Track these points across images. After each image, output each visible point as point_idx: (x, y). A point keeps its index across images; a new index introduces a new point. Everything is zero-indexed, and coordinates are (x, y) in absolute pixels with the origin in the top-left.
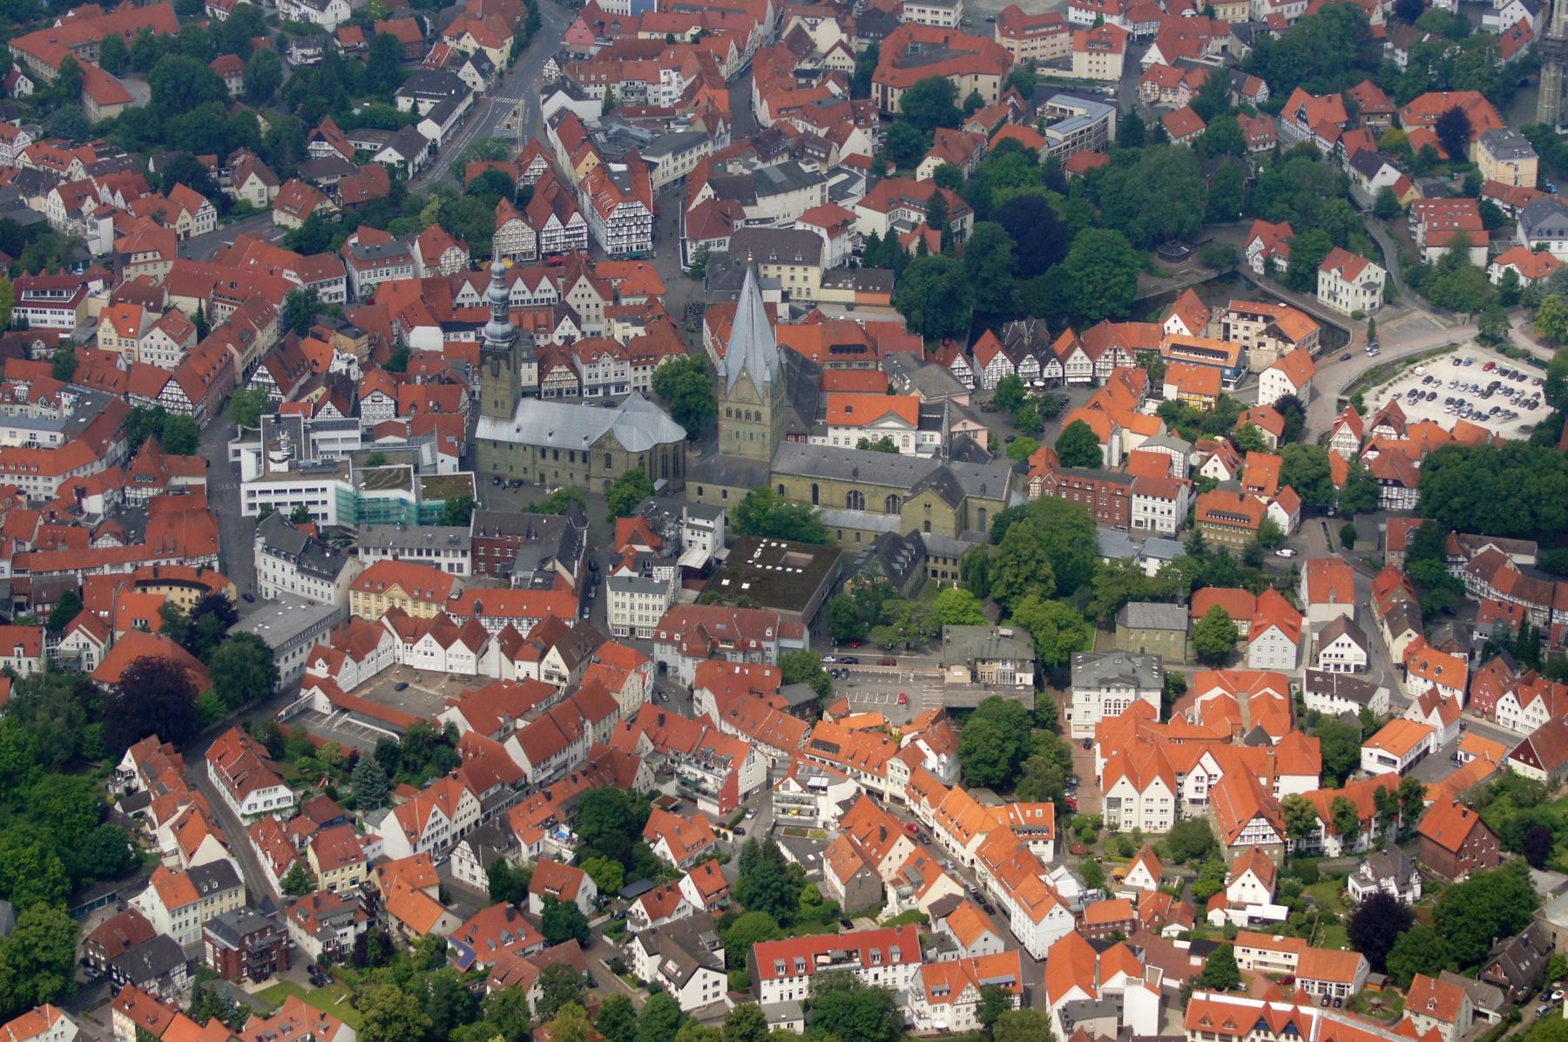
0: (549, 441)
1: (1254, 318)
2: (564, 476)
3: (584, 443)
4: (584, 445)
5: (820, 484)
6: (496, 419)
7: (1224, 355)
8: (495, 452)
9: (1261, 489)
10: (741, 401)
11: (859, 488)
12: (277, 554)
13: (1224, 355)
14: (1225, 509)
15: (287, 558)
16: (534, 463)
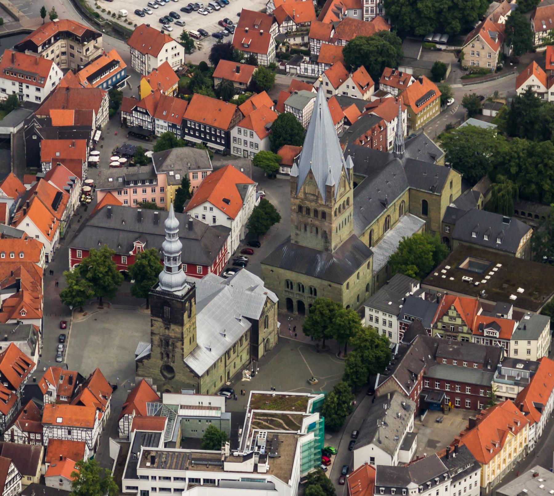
0: (229, 340)
1: (48, 43)
2: (238, 361)
3: (241, 323)
4: (245, 326)
5: (374, 227)
6: (192, 354)
7: (113, 63)
8: (207, 379)
9: (368, 85)
10: (342, 196)
11: (388, 213)
12: (434, 483)
13: (113, 63)
14: (420, 96)
15: (442, 479)
16: (226, 366)
